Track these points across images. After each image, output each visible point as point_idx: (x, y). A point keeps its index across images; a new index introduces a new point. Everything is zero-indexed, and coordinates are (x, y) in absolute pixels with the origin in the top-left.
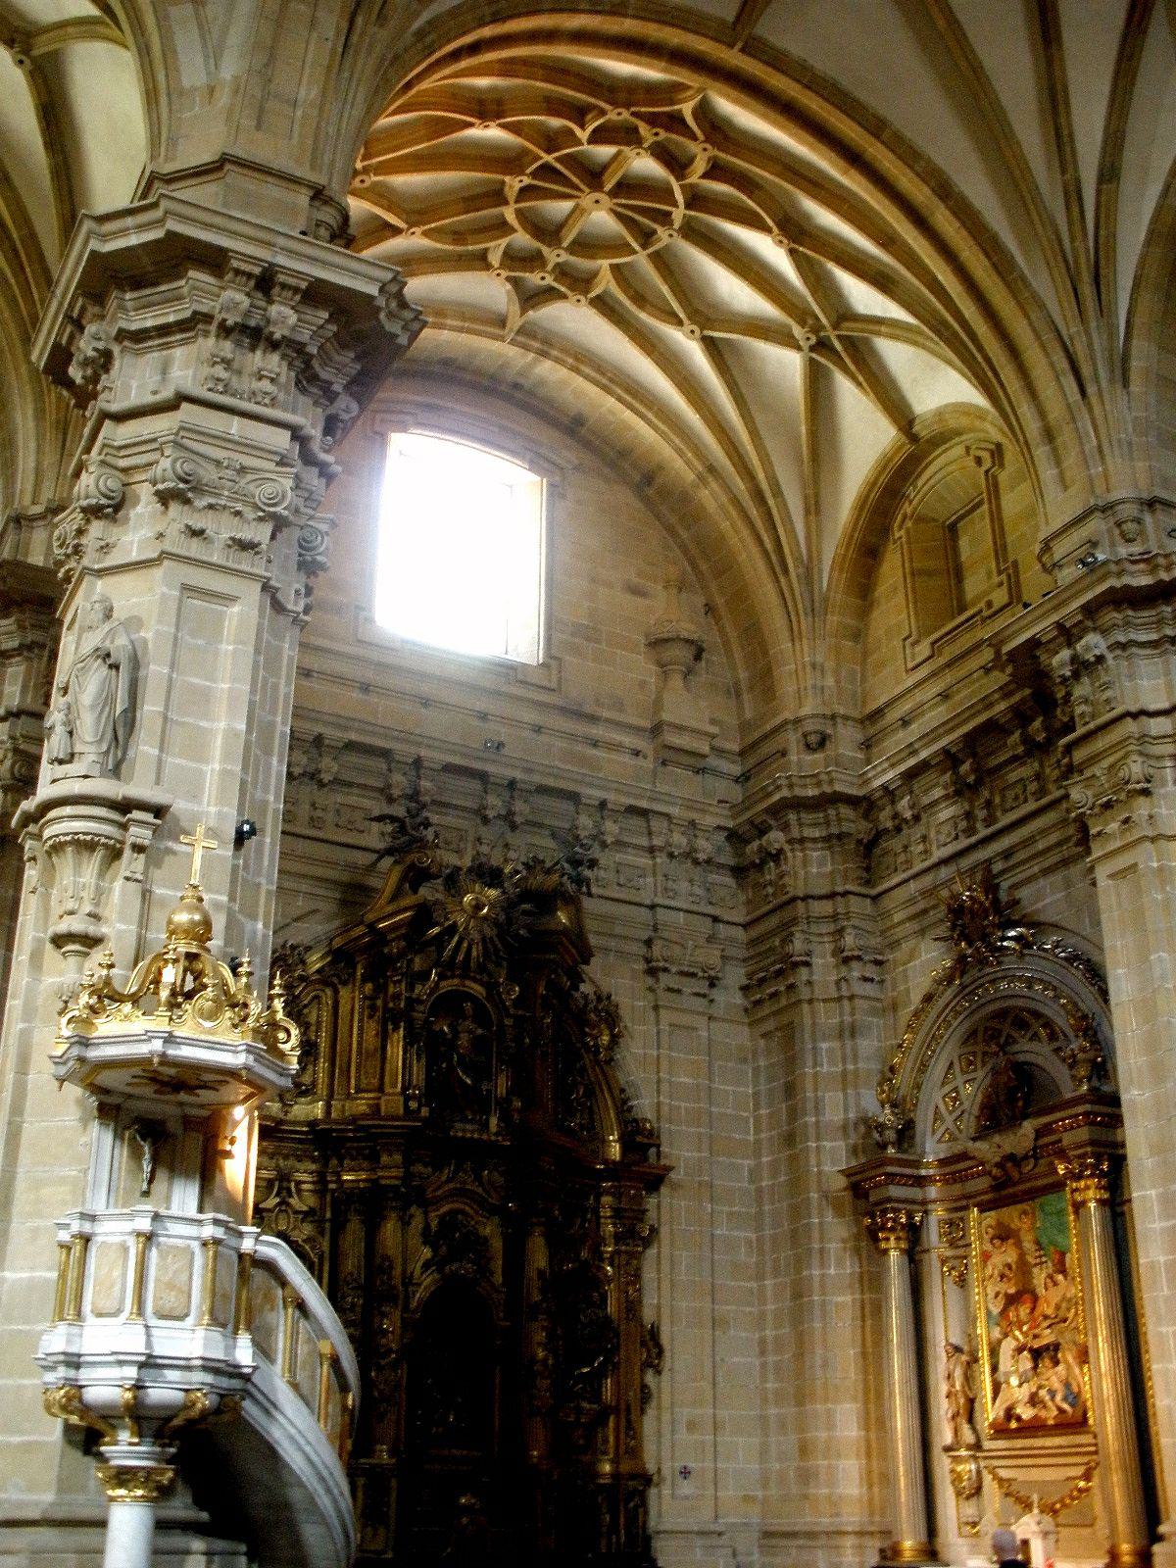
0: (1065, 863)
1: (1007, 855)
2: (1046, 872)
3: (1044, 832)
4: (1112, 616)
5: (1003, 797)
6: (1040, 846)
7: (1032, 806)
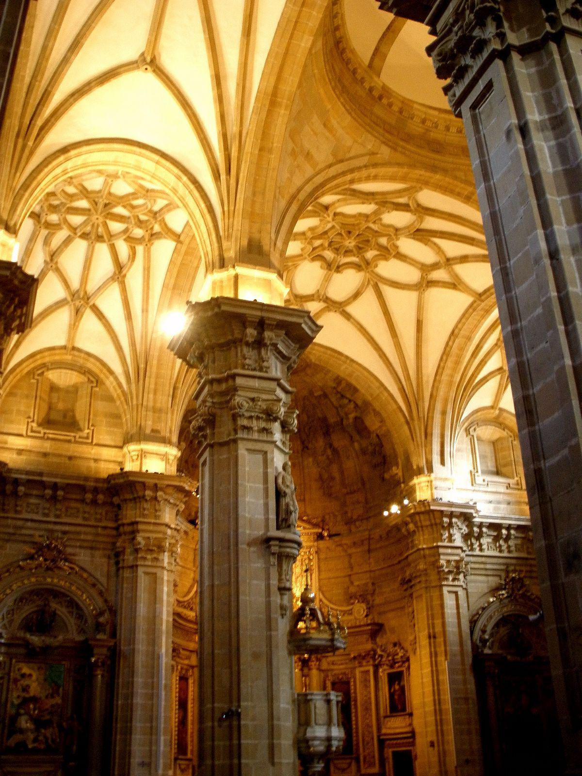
0: (92, 548)
1: (65, 533)
2: (81, 547)
3: (85, 533)
4: (170, 490)
5: (67, 510)
6: (82, 537)
7: (79, 521)
